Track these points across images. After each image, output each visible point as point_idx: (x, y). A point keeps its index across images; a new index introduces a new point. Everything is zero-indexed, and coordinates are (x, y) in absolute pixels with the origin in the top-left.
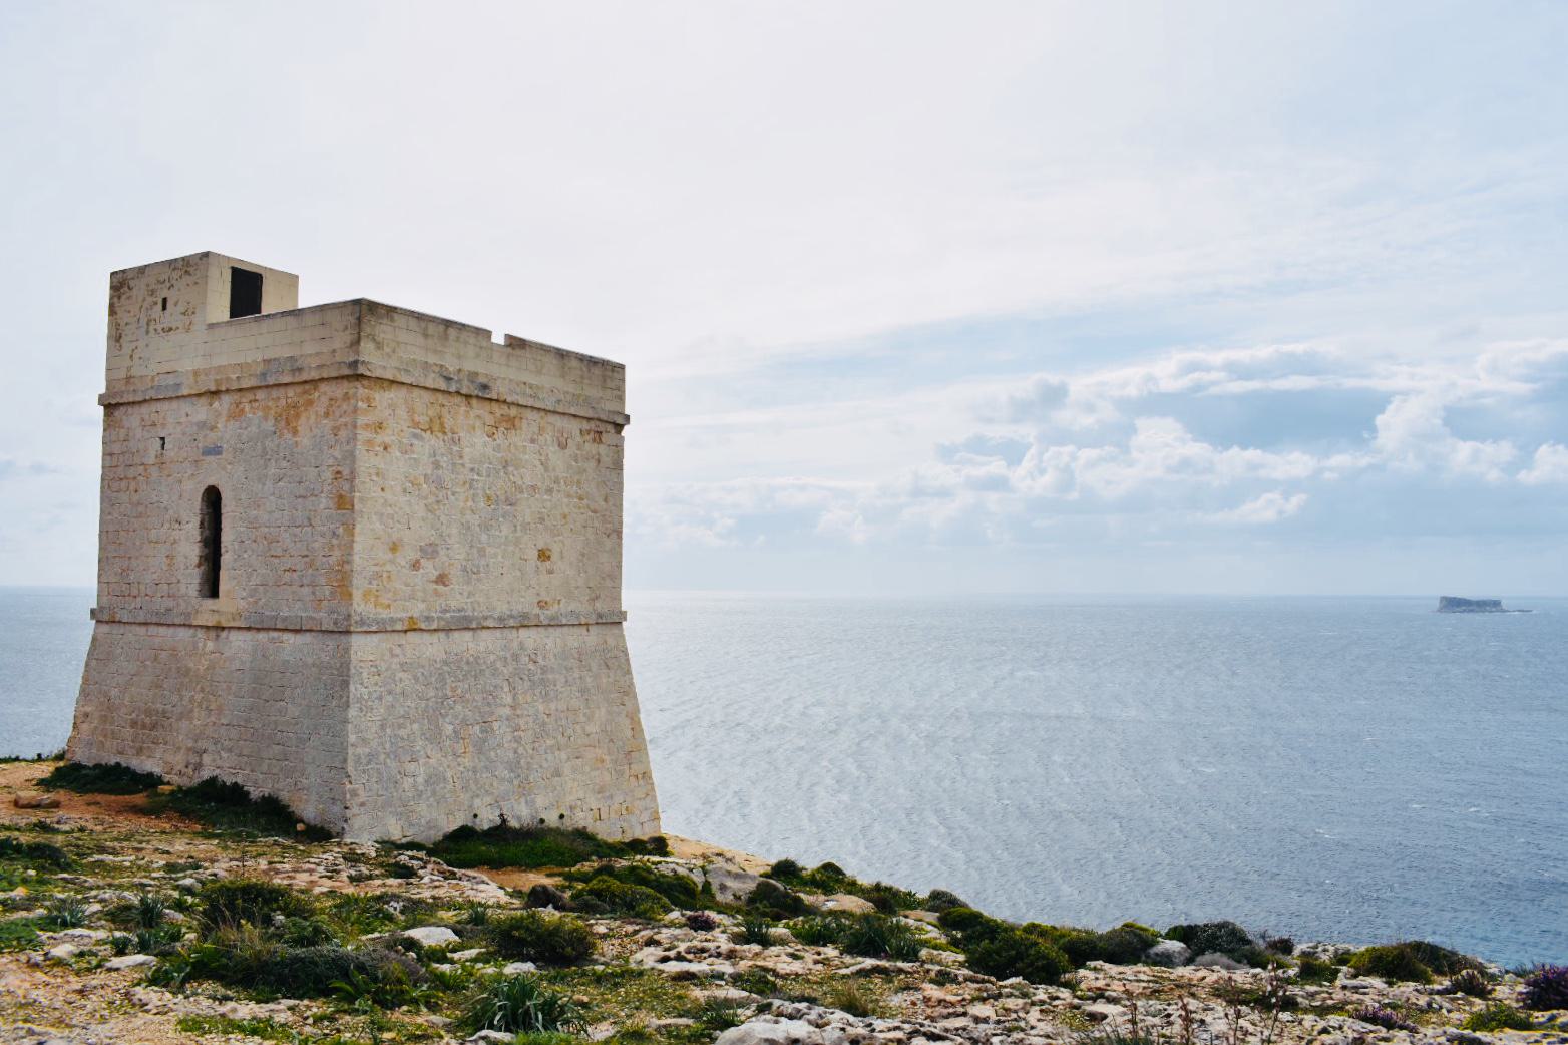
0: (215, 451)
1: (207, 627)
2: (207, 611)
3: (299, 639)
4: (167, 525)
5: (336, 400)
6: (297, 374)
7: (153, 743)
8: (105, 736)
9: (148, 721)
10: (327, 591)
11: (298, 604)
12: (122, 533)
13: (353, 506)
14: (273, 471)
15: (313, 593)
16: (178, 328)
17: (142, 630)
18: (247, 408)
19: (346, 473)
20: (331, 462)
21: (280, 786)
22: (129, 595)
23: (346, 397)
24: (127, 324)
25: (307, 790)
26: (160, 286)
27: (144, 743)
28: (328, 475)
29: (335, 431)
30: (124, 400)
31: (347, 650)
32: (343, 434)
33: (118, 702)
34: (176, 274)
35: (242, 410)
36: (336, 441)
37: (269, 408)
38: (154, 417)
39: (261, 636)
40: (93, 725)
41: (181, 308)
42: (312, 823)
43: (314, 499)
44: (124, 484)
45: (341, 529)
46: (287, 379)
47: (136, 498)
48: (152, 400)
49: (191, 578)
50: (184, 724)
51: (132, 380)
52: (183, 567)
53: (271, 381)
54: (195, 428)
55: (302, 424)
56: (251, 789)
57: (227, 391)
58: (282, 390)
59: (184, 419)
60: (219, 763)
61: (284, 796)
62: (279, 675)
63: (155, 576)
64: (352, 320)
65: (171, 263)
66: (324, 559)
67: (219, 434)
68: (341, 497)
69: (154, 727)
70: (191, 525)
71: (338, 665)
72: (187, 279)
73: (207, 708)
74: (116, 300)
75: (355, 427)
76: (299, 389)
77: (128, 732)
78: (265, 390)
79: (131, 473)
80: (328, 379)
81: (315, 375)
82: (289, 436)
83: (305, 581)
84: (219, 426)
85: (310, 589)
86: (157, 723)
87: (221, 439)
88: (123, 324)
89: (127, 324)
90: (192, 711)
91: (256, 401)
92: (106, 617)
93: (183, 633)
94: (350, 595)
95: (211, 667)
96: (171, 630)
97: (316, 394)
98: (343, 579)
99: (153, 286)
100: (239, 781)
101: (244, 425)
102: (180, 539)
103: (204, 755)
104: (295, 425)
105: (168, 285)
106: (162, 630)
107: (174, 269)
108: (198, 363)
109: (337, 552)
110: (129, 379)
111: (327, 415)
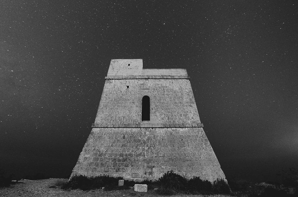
2: (145, 123)
7: (125, 166)
8: (97, 166)
9: (121, 158)
46: (170, 78)
69: (125, 160)
86: (127, 159)
93: (134, 130)
103: (154, 169)
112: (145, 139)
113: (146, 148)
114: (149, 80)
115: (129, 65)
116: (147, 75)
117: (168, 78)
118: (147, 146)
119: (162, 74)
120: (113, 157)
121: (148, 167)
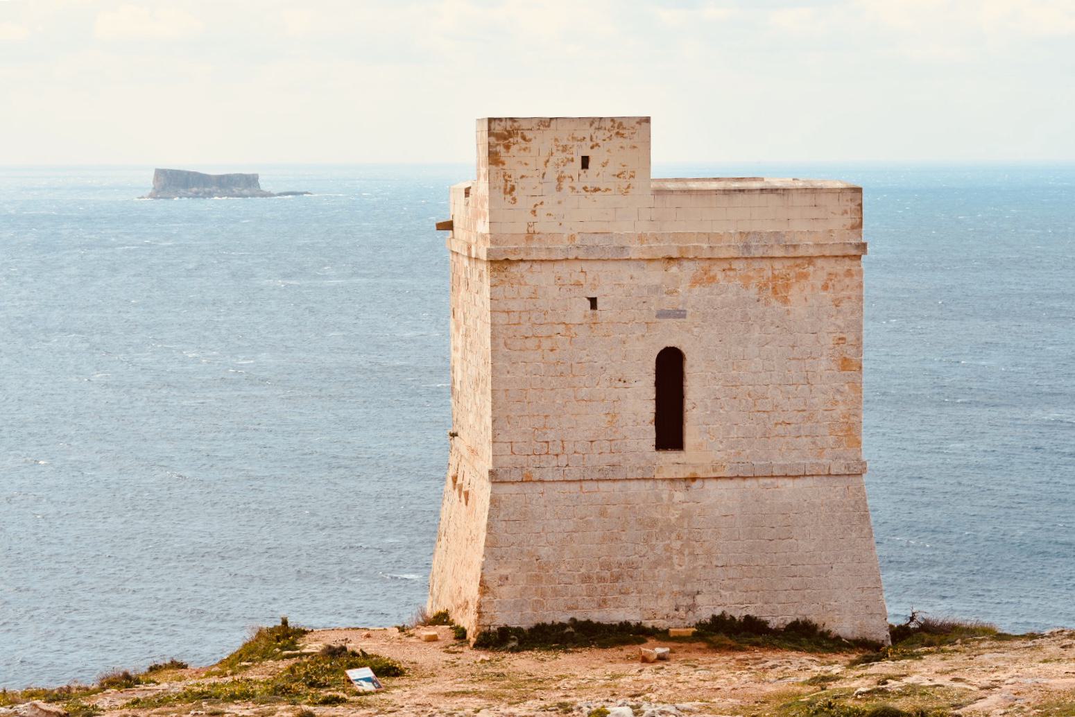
0: (680, 314)
1: (672, 480)
3: (797, 481)
5: (836, 275)
6: (791, 249)
8: (543, 595)
9: (607, 574)
10: (831, 440)
11: (795, 453)
12: (532, 392)
13: (861, 368)
14: (757, 335)
15: (814, 443)
16: (607, 190)
17: (574, 487)
18: (720, 276)
19: (851, 338)
20: (832, 329)
21: (803, 611)
22: (547, 453)
23: (849, 273)
24: (522, 177)
25: (839, 610)
26: (576, 143)
27: (606, 595)
29: (837, 303)
30: (534, 256)
31: (860, 489)
32: (845, 306)
33: (552, 560)
34: (600, 134)
35: (713, 279)
36: (839, 312)
37: (750, 278)
38: (582, 278)
39: (748, 483)
40: (519, 587)
41: (613, 168)
42: (850, 636)
43: (811, 361)
44: (531, 343)
45: (846, 387)
46: (779, 253)
47: (552, 357)
48: (576, 259)
49: (650, 434)
50: (663, 572)
51: (536, 237)
52: (630, 423)
54: (646, 291)
55: (794, 294)
56: (768, 619)
57: (695, 259)
59: (626, 281)
60: (720, 601)
61: (815, 619)
62: (780, 517)
63: (587, 434)
64: (853, 206)
66: (826, 413)
67: (681, 299)
68: (845, 359)
69: (617, 578)
70: (640, 384)
71: (853, 503)
72: (617, 141)
73: (691, 554)
74: (501, 149)
75: (861, 300)
76: (788, 263)
77: (580, 588)
78: (744, 261)
79: (543, 331)
80: (824, 256)
83: (802, 432)
84: (680, 290)
85: (809, 439)
86: (621, 575)
87: (684, 303)
88: (516, 175)
89: (522, 177)
90: (670, 558)
91: (730, 269)
92: (516, 476)
93: (634, 486)
94: (859, 443)
95: (686, 515)
96: (618, 485)
97: (811, 269)
98: (850, 429)
99: (565, 142)
100: (752, 612)
101: (715, 291)
102: (626, 397)
103: (699, 598)
104: (784, 294)
105: (591, 144)
106: (602, 485)
107: (599, 129)
108: (644, 228)
109: (841, 408)
110: (530, 236)
111: (825, 287)
113: (677, 545)
114: (685, 263)
115: (585, 162)
116: (676, 237)
117: (770, 253)
118: (679, 537)
119: (745, 227)
120: (583, 570)
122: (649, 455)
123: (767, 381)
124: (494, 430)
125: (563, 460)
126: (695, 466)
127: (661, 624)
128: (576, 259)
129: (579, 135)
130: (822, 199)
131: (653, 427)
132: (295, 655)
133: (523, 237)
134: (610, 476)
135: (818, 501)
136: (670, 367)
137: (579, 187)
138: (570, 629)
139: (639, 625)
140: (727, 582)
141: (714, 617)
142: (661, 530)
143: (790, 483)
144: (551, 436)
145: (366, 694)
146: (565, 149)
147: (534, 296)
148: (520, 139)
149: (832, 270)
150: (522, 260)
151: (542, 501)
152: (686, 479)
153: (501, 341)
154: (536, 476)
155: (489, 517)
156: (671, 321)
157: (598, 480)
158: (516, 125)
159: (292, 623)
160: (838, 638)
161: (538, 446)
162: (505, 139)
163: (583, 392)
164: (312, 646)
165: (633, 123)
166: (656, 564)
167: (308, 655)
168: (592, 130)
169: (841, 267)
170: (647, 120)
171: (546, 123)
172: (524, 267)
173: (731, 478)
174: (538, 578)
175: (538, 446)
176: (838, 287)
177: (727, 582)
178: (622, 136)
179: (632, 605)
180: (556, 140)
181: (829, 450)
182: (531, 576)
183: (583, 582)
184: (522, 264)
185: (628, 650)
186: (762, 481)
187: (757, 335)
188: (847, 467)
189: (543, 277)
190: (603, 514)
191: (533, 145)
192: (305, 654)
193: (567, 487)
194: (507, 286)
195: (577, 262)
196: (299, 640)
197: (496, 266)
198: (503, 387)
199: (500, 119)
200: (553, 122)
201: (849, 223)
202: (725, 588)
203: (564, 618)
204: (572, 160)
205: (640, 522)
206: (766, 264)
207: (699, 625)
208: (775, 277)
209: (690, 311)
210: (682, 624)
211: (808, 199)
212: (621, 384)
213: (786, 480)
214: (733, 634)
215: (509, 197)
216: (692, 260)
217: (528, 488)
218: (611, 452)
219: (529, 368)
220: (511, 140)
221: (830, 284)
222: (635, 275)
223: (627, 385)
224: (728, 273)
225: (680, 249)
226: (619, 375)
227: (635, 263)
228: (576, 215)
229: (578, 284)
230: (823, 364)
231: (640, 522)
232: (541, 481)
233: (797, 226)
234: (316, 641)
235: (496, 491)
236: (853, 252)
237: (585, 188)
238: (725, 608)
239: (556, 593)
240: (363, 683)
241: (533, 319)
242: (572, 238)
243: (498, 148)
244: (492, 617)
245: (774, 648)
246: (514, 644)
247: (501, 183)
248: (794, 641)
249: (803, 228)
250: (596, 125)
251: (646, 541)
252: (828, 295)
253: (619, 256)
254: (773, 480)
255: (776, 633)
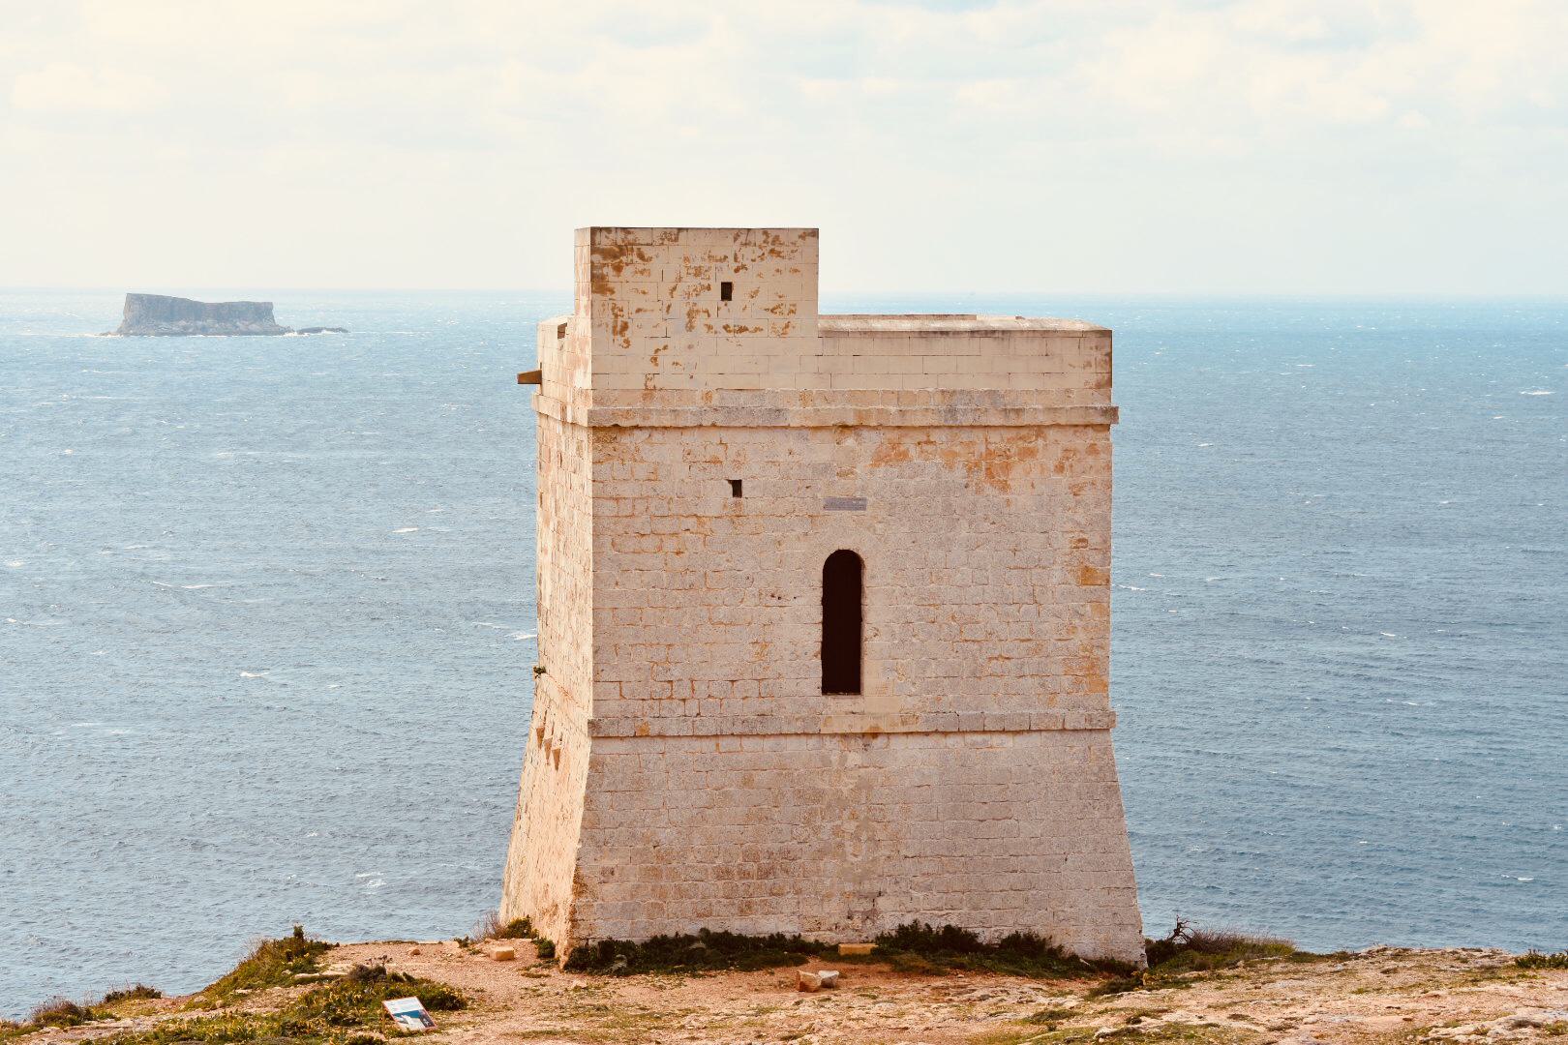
0: (856, 504)
1: (845, 736)
3: (1018, 739)
4: (750, 602)
5: (1075, 452)
9: (752, 867)
10: (1066, 682)
12: (650, 611)
14: (964, 534)
16: (757, 329)
17: (708, 745)
18: (913, 452)
19: (1094, 539)
20: (1069, 526)
21: (1026, 920)
22: (670, 698)
23: (1093, 450)
26: (713, 264)
28: (1064, 543)
29: (1076, 491)
30: (654, 421)
32: (1088, 495)
33: (676, 847)
34: (748, 253)
35: (904, 455)
36: (1078, 502)
37: (955, 454)
38: (720, 453)
39: (951, 741)
40: (629, 885)
41: (766, 300)
42: (1091, 956)
44: (648, 543)
48: (714, 425)
49: (814, 671)
50: (830, 864)
51: (657, 394)
53: (968, 420)
55: (1017, 476)
58: (980, 434)
60: (910, 906)
61: (1041, 931)
63: (726, 670)
64: (1099, 356)
65: (741, 235)
67: (859, 482)
69: (765, 874)
71: (1096, 769)
72: (772, 262)
74: (608, 271)
76: (1013, 433)
77: (715, 887)
79: (665, 526)
80: (1059, 425)
81: (1043, 419)
82: (989, 490)
87: (863, 489)
90: (841, 845)
92: (627, 729)
93: (792, 745)
95: (864, 786)
96: (769, 743)
97: (1040, 442)
99: (698, 263)
100: (954, 923)
101: (908, 472)
103: (880, 901)
105: (735, 265)
106: (747, 743)
108: (807, 383)
109: (1080, 638)
110: (649, 393)
111: (1060, 469)
112: (846, 786)
113: (850, 826)
114: (865, 433)
115: (727, 291)
117: (984, 421)
118: (854, 816)
119: (948, 384)
120: (719, 862)
121: (861, 896)
122: (812, 701)
123: (979, 599)
124: (596, 665)
125: (692, 707)
126: (875, 717)
127: (827, 937)
128: (714, 425)
129: (719, 253)
130: (1056, 346)
131: (818, 661)
132: (313, 980)
133: (639, 394)
134: (759, 729)
135: (1047, 767)
136: (843, 577)
137: (718, 324)
138: (701, 945)
139: (797, 939)
140: (919, 879)
141: (901, 928)
142: (829, 806)
143: (1009, 741)
144: (676, 673)
145: (412, 1034)
146: (698, 272)
147: (653, 477)
148: (636, 259)
149: (1068, 445)
150: (637, 427)
151: (662, 765)
152: (864, 735)
153: (607, 540)
154: (654, 730)
155: (588, 786)
156: (846, 513)
157: (741, 736)
158: (630, 237)
159: (313, 933)
160: (1074, 957)
161: (657, 687)
162: (615, 257)
163: (722, 613)
164: (338, 967)
165: (795, 237)
166: (822, 853)
167: (330, 979)
168: (736, 247)
169: (1081, 441)
170: (815, 233)
171: (672, 235)
172: (640, 436)
173: (927, 734)
174: (656, 873)
175: (657, 687)
176: (1078, 468)
177: (919, 879)
178: (779, 254)
179: (787, 911)
180: (686, 259)
181: (1063, 695)
182: (647, 869)
183: (719, 878)
184: (637, 432)
185: (781, 974)
186: (970, 738)
187: (964, 534)
188: (1089, 719)
189: (666, 451)
190: (747, 782)
191: (655, 266)
192: (326, 978)
193: (697, 744)
194: (616, 463)
195: (713, 430)
196: (319, 959)
197: (601, 434)
198: (609, 605)
199: (608, 230)
200: (682, 235)
201: (1093, 379)
202: (918, 887)
203: (692, 929)
204: (709, 288)
205: (799, 794)
206: (978, 436)
207: (881, 939)
208: (990, 453)
209: (871, 500)
210: (856, 938)
211: (1036, 346)
212: (775, 601)
213: (1003, 737)
214: (930, 952)
215: (620, 339)
216: (875, 428)
217: (643, 746)
218: (760, 696)
219: (646, 577)
220: (624, 259)
221: (1067, 464)
222: (796, 450)
223: (783, 602)
224: (926, 447)
225: (859, 414)
226: (772, 589)
227: (795, 433)
228: (709, 364)
229: (716, 461)
230: (1057, 575)
231: (800, 795)
232: (661, 736)
233: (1023, 383)
234: (343, 959)
235: (599, 750)
236: (1099, 420)
237: (726, 327)
238: (917, 916)
239: (681, 893)
240: (408, 1019)
241: (652, 509)
242: (708, 396)
243: (605, 270)
244: (591, 927)
245: (985, 971)
246: (620, 964)
247: (609, 319)
248: (1012, 962)
249: (1030, 385)
250: (742, 239)
251: (808, 822)
252: (1064, 480)
253: (774, 423)
254: (986, 737)
255: (987, 950)
